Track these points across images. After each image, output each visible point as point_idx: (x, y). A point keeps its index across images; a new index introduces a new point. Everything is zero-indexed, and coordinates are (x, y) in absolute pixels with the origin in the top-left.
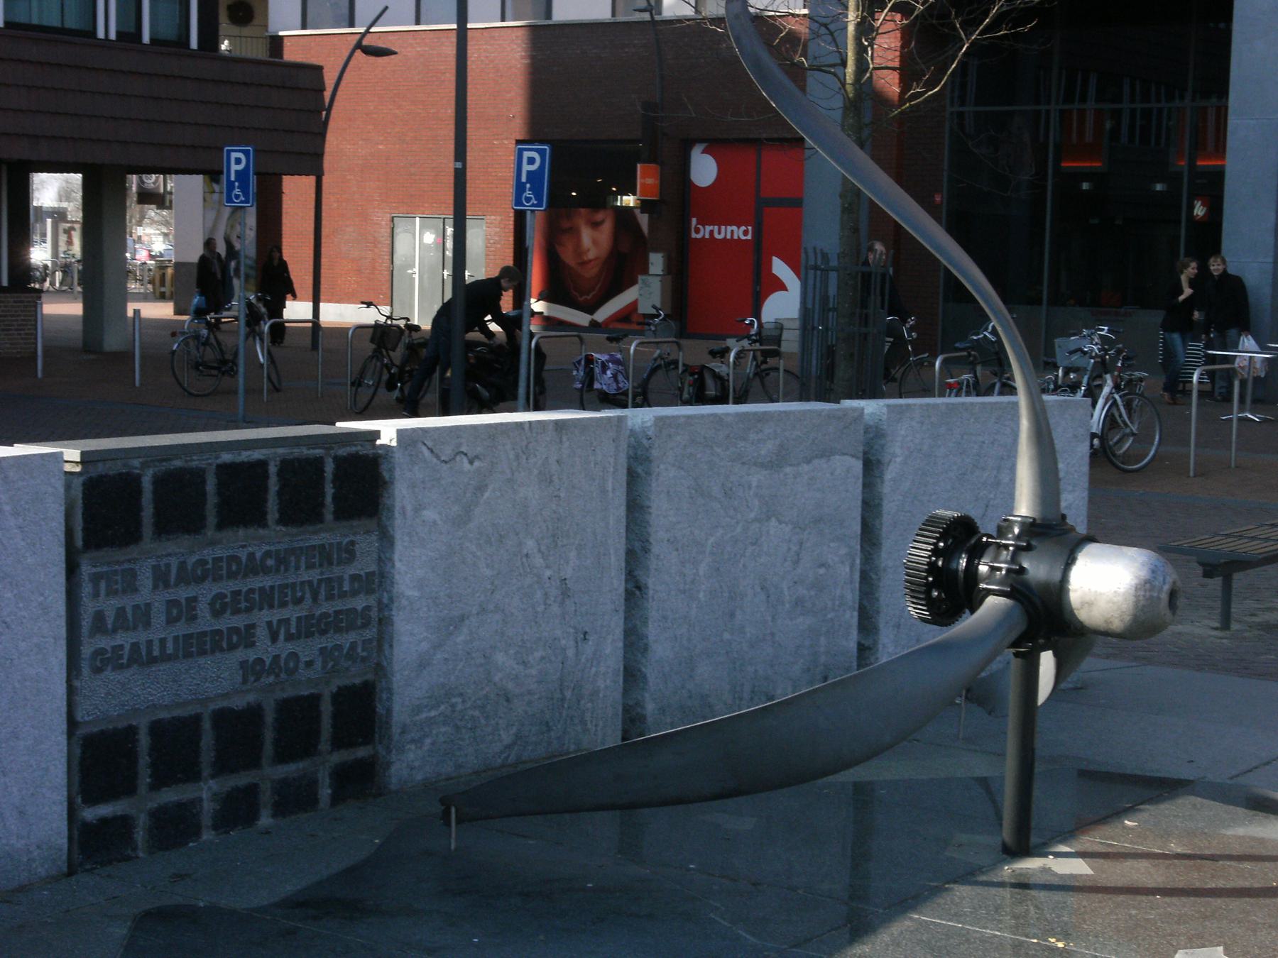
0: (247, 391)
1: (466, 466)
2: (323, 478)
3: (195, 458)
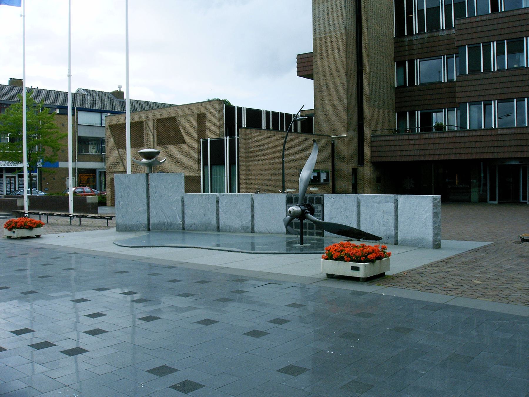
1: (333, 199)
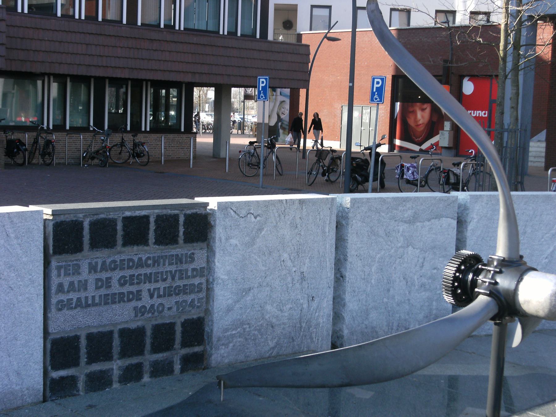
0: (264, 175)
1: (253, 219)
2: (178, 224)
3: (111, 214)
